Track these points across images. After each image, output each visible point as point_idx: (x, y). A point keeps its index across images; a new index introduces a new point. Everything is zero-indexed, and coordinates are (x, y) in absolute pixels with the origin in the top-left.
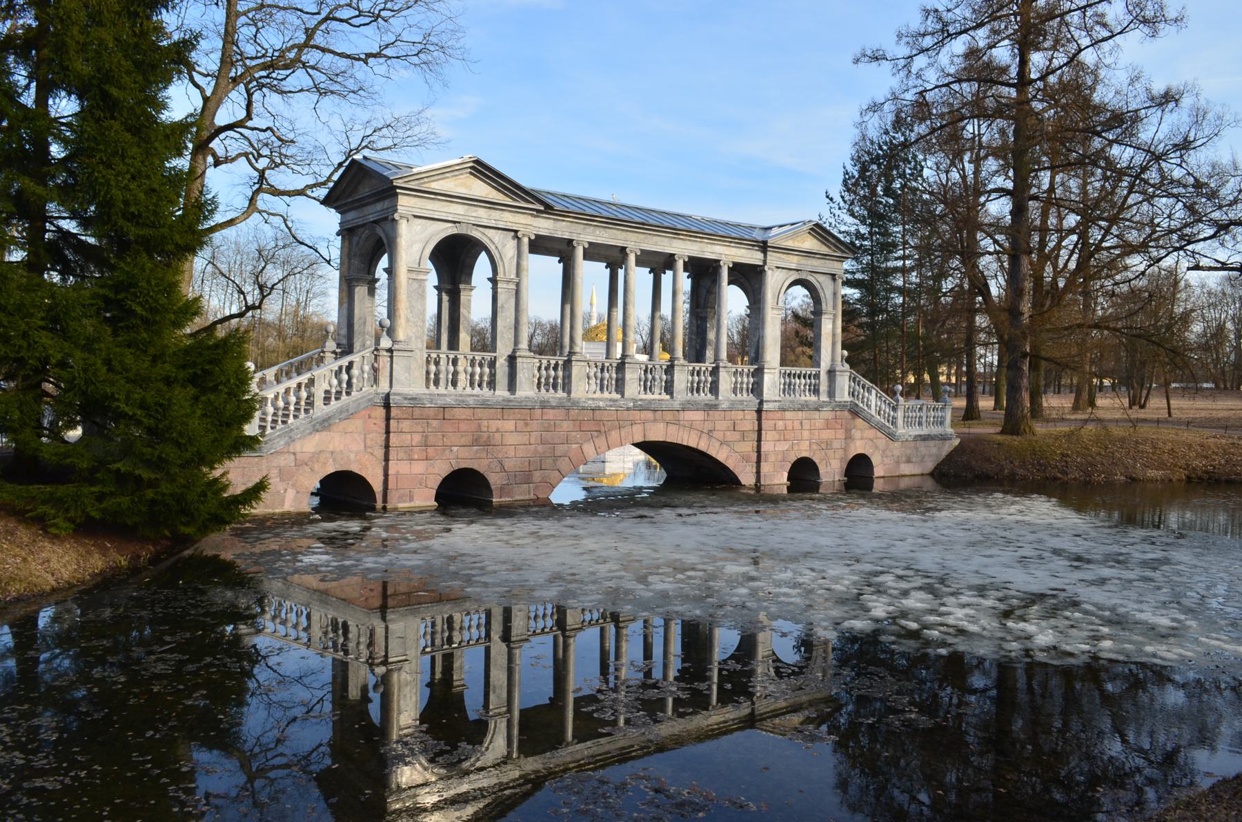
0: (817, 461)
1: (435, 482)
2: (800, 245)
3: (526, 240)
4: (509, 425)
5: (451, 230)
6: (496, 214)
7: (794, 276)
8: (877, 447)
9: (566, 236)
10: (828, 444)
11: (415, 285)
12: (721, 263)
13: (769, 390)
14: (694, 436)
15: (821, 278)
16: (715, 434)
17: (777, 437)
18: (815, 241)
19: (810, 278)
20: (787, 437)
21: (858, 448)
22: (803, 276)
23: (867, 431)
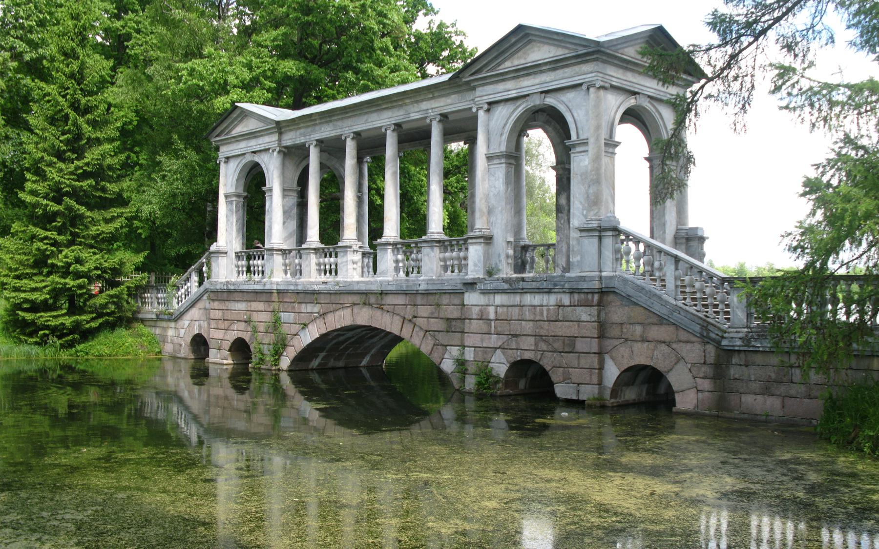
0: (548, 368)
1: (227, 345)
2: (522, 61)
3: (275, 153)
4: (261, 306)
5: (244, 162)
6: (260, 141)
7: (522, 107)
8: (680, 359)
9: (302, 140)
10: (569, 345)
11: (230, 206)
12: (428, 121)
13: (475, 265)
14: (397, 321)
15: (570, 96)
16: (419, 321)
17: (485, 328)
18: (546, 48)
19: (550, 101)
20: (499, 329)
21: (641, 355)
22: (536, 101)
23: (655, 328)
